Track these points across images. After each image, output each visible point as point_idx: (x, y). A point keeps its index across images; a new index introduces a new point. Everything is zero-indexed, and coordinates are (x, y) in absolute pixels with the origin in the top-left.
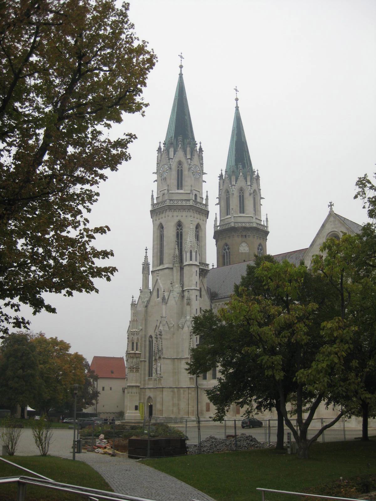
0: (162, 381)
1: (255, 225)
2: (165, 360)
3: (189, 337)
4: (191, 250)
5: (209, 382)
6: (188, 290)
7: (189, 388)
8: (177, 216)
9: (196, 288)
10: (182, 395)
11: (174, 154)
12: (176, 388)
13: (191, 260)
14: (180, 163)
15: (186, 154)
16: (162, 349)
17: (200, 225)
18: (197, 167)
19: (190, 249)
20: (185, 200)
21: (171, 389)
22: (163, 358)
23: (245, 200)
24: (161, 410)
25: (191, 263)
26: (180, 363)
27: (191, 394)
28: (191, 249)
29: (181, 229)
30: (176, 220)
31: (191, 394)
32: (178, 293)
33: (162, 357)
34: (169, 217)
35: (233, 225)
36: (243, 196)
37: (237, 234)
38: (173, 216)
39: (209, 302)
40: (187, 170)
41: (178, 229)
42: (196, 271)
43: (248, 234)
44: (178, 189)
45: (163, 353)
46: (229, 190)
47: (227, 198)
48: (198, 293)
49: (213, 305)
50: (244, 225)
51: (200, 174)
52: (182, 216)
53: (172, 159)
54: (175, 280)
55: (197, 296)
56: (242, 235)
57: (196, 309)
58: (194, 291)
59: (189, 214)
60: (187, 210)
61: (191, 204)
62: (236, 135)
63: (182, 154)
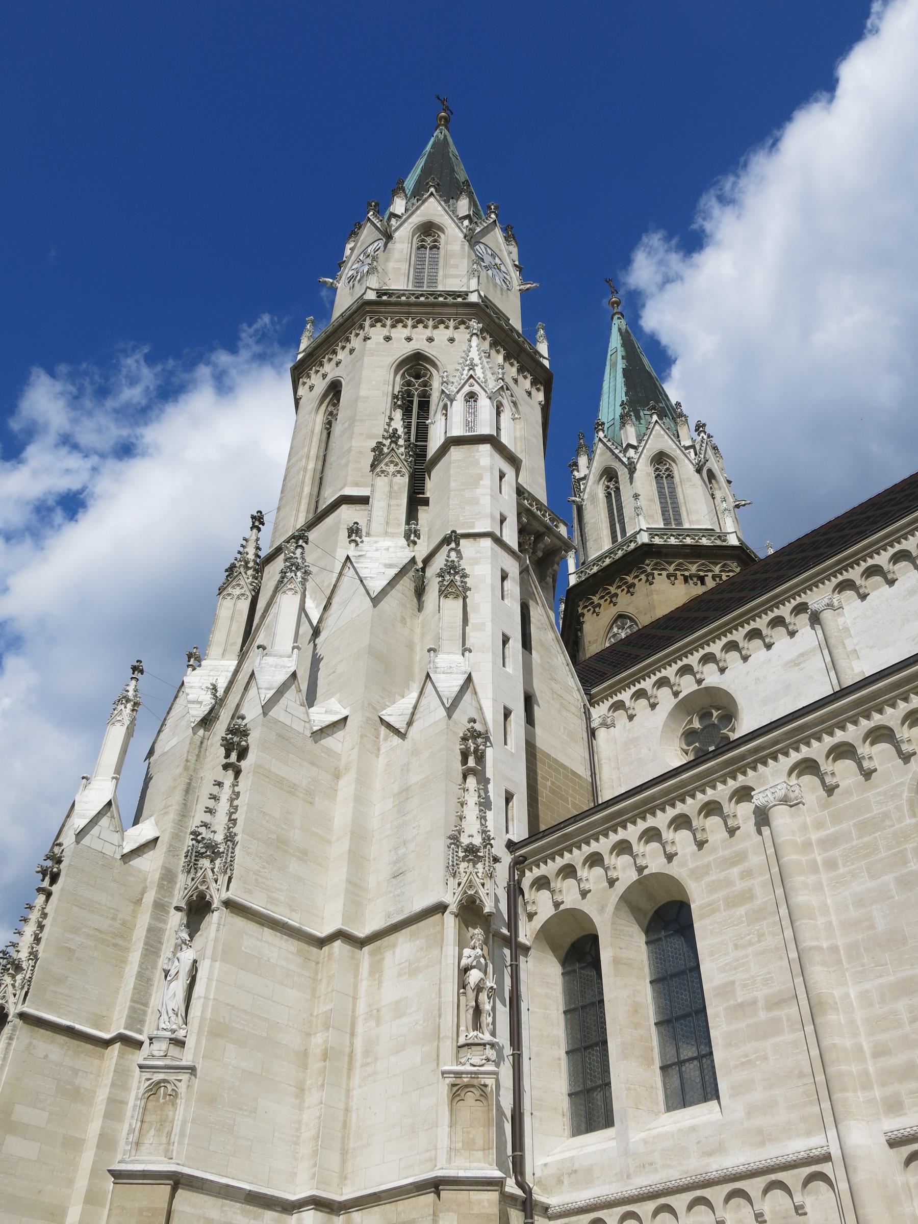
0: (181, 1113)
1: (733, 541)
2: (239, 922)
3: (459, 768)
6: (452, 539)
7: (436, 1185)
14: (429, 229)
16: (230, 838)
19: (467, 389)
22: (229, 904)
23: (679, 490)
26: (376, 969)
28: (476, 389)
30: (401, 348)
32: (390, 566)
34: (369, 341)
35: (644, 538)
36: (670, 476)
37: (664, 573)
38: (388, 339)
39: (577, 695)
40: (460, 243)
42: (502, 476)
43: (710, 574)
45: (228, 867)
46: (616, 465)
47: (608, 496)
49: (599, 712)
50: (688, 541)
53: (399, 217)
54: (375, 527)
55: (504, 577)
56: (686, 579)
60: (452, 324)
62: (623, 358)
63: (440, 208)
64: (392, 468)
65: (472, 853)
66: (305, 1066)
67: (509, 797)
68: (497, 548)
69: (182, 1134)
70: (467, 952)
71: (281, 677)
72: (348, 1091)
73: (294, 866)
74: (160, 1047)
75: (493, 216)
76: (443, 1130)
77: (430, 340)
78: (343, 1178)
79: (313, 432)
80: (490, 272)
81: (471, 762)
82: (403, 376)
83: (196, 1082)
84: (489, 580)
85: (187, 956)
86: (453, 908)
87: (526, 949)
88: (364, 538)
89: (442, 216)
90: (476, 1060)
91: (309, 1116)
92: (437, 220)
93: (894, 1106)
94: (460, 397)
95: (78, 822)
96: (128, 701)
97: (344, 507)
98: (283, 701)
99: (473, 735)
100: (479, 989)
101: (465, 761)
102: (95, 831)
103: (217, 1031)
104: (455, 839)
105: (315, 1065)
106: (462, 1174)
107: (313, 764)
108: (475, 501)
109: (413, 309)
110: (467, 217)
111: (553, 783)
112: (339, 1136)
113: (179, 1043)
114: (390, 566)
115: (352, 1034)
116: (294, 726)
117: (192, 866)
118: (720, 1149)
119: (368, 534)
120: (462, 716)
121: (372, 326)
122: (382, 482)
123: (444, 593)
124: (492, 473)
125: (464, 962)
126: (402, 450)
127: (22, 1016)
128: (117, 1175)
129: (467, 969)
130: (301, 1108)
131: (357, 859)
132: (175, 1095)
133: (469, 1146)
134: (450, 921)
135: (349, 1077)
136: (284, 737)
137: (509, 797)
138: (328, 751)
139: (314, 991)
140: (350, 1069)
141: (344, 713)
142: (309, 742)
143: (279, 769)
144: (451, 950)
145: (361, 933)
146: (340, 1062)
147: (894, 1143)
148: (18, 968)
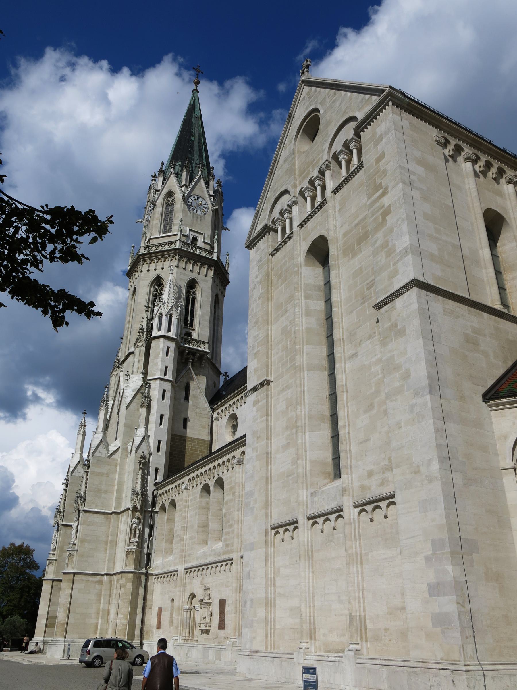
0: (75, 560)
2: (87, 514)
4: (161, 314)
5: (165, 561)
7: (122, 573)
8: (155, 270)
9: (162, 377)
10: (115, 591)
11: (163, 184)
12: (107, 575)
13: (160, 329)
14: (170, 194)
15: (179, 180)
17: (197, 283)
18: (201, 199)
19: (160, 311)
20: (169, 243)
21: (98, 578)
22: (84, 511)
24: (63, 624)
25: (160, 333)
27: (125, 586)
29: (162, 289)
30: (153, 275)
31: (125, 586)
33: (82, 508)
40: (180, 202)
41: (156, 290)
42: (168, 348)
44: (165, 232)
48: (168, 386)
49: (215, 415)
51: (206, 210)
52: (163, 268)
53: (158, 191)
54: (135, 370)
55: (164, 391)
57: (162, 416)
58: (158, 381)
59: (175, 263)
61: (177, 245)
63: (174, 181)
64: (141, 343)
65: (137, 494)
66: (107, 544)
67: (157, 470)
68: (162, 382)
69: (75, 564)
70: (134, 520)
71: (98, 442)
72: (116, 549)
73: (103, 495)
74: (71, 546)
75: (200, 172)
76: (124, 561)
77: (163, 268)
78: (114, 568)
79: (131, 309)
80: (195, 211)
81: (141, 466)
82: (154, 287)
83: (78, 553)
84: (157, 397)
85: (76, 523)
86: (131, 509)
87: (157, 512)
88: (131, 376)
89: (174, 186)
90: (132, 546)
91: (107, 555)
92: (173, 190)
93: (185, 562)
94: (157, 316)
95: (71, 469)
96: (82, 426)
97: (131, 355)
98: (98, 450)
99: (143, 457)
100: (135, 529)
101: (140, 466)
102: (76, 471)
103: (82, 541)
104: (133, 491)
105: (109, 544)
106: (126, 571)
107: (109, 465)
108: (156, 364)
109: (157, 254)
110: (185, 185)
111: (192, 447)
112: (113, 560)
113: (75, 544)
114: (134, 390)
115: (117, 536)
116: (102, 456)
117: (76, 502)
118: (170, 566)
119: (132, 374)
120: (140, 451)
121: (143, 264)
122: (138, 349)
123: (142, 406)
124: (163, 351)
125: (132, 522)
126: (145, 333)
127: (62, 525)
128: (64, 573)
129: (133, 524)
130: (106, 554)
131: (120, 491)
132: (74, 556)
133: (129, 564)
134: (130, 512)
135: (116, 546)
136: (99, 460)
137: (157, 470)
138: (114, 459)
139: (109, 526)
140: (116, 544)
141: (119, 445)
142: (108, 460)
143: (97, 470)
144: (130, 519)
145: (119, 511)
146: (114, 543)
147: (185, 569)
148: (60, 512)
